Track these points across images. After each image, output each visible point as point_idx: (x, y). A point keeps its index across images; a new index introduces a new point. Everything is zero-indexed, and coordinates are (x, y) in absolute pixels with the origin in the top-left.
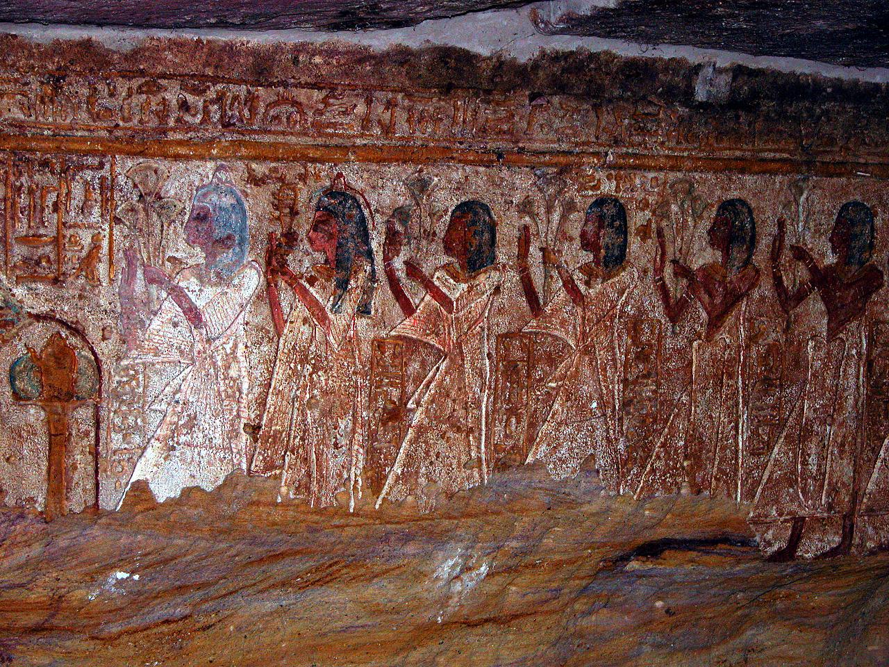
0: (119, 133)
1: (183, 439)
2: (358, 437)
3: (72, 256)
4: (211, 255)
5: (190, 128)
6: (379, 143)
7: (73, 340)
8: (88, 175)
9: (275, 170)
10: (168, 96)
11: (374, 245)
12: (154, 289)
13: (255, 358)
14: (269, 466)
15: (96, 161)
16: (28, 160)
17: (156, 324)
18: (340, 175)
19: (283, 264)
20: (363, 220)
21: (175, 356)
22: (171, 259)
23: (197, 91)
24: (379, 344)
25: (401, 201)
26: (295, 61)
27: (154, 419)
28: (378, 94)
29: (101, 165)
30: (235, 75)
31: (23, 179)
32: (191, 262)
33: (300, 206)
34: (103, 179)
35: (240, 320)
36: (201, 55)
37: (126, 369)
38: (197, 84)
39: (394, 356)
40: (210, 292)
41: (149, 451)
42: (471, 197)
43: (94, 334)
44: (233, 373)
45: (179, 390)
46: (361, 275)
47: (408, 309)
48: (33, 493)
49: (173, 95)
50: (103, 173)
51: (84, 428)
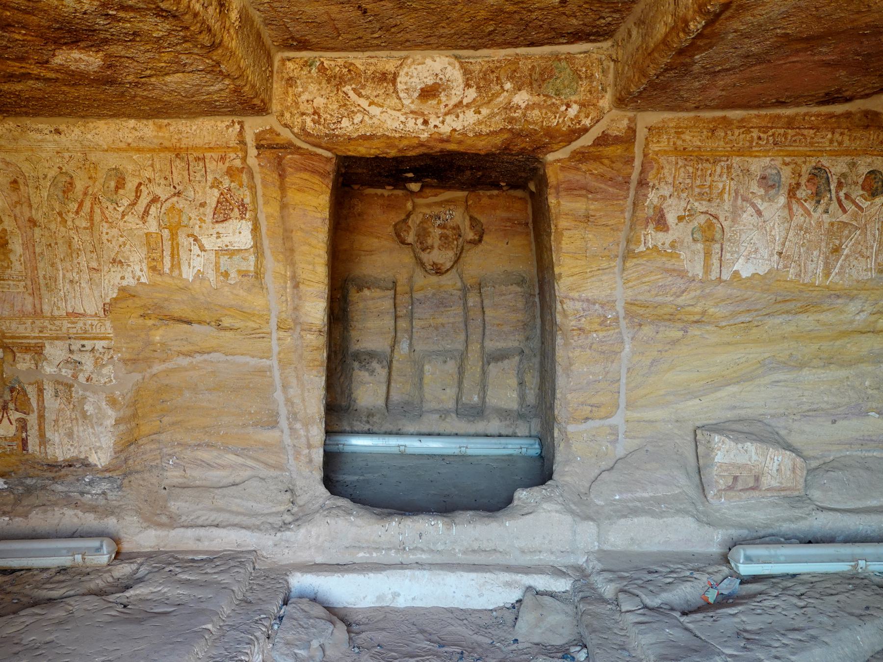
0: (734, 149)
1: (753, 256)
2: (821, 258)
3: (715, 192)
4: (766, 192)
5: (761, 146)
6: (836, 149)
7: (715, 221)
8: (722, 163)
9: (793, 160)
10: (753, 134)
11: (832, 187)
12: (744, 203)
13: (781, 229)
14: (785, 267)
15: (725, 159)
16: (701, 159)
17: (745, 215)
18: (819, 161)
19: (795, 195)
20: (828, 178)
21: (751, 227)
22: (752, 193)
23: (764, 132)
24: (832, 224)
25: (844, 171)
26: (804, 119)
27: (742, 249)
28: (838, 130)
29: (727, 160)
30: (779, 125)
31: (700, 165)
32: (759, 194)
33: (803, 173)
34: (728, 165)
35: (777, 215)
36: (767, 119)
37: (733, 231)
38: (764, 129)
39: (838, 228)
40: (766, 204)
41: (740, 261)
42: (874, 168)
43: (722, 219)
44: (773, 233)
45: (752, 239)
46: (826, 198)
47: (845, 211)
48: (698, 272)
49: (755, 134)
50: (729, 162)
51: (717, 251)
